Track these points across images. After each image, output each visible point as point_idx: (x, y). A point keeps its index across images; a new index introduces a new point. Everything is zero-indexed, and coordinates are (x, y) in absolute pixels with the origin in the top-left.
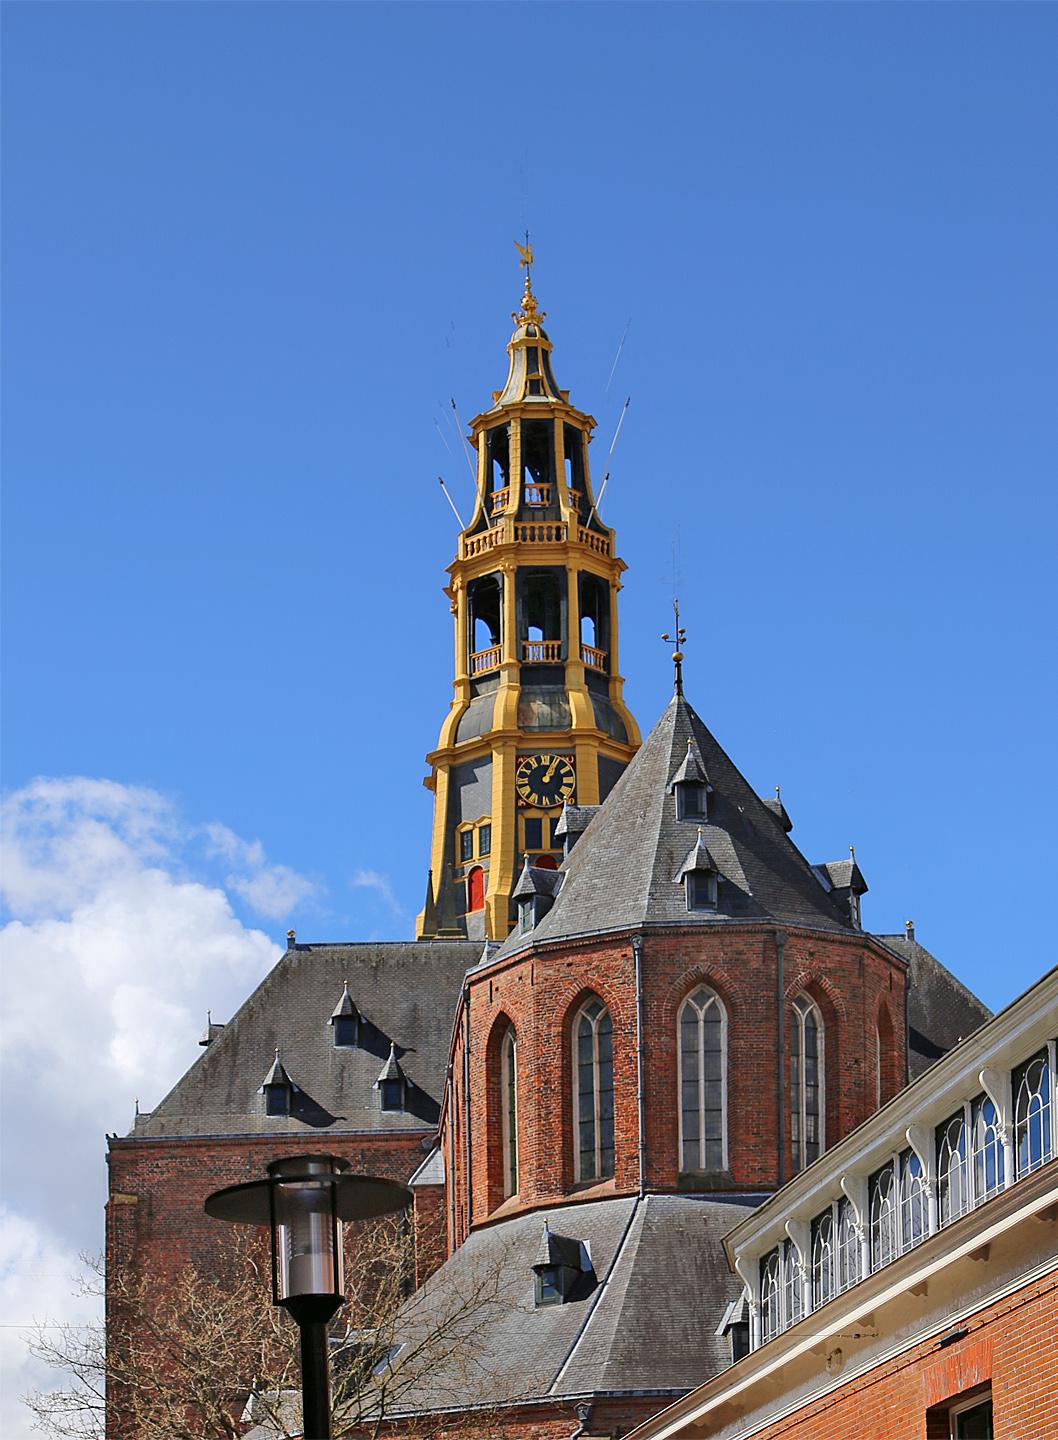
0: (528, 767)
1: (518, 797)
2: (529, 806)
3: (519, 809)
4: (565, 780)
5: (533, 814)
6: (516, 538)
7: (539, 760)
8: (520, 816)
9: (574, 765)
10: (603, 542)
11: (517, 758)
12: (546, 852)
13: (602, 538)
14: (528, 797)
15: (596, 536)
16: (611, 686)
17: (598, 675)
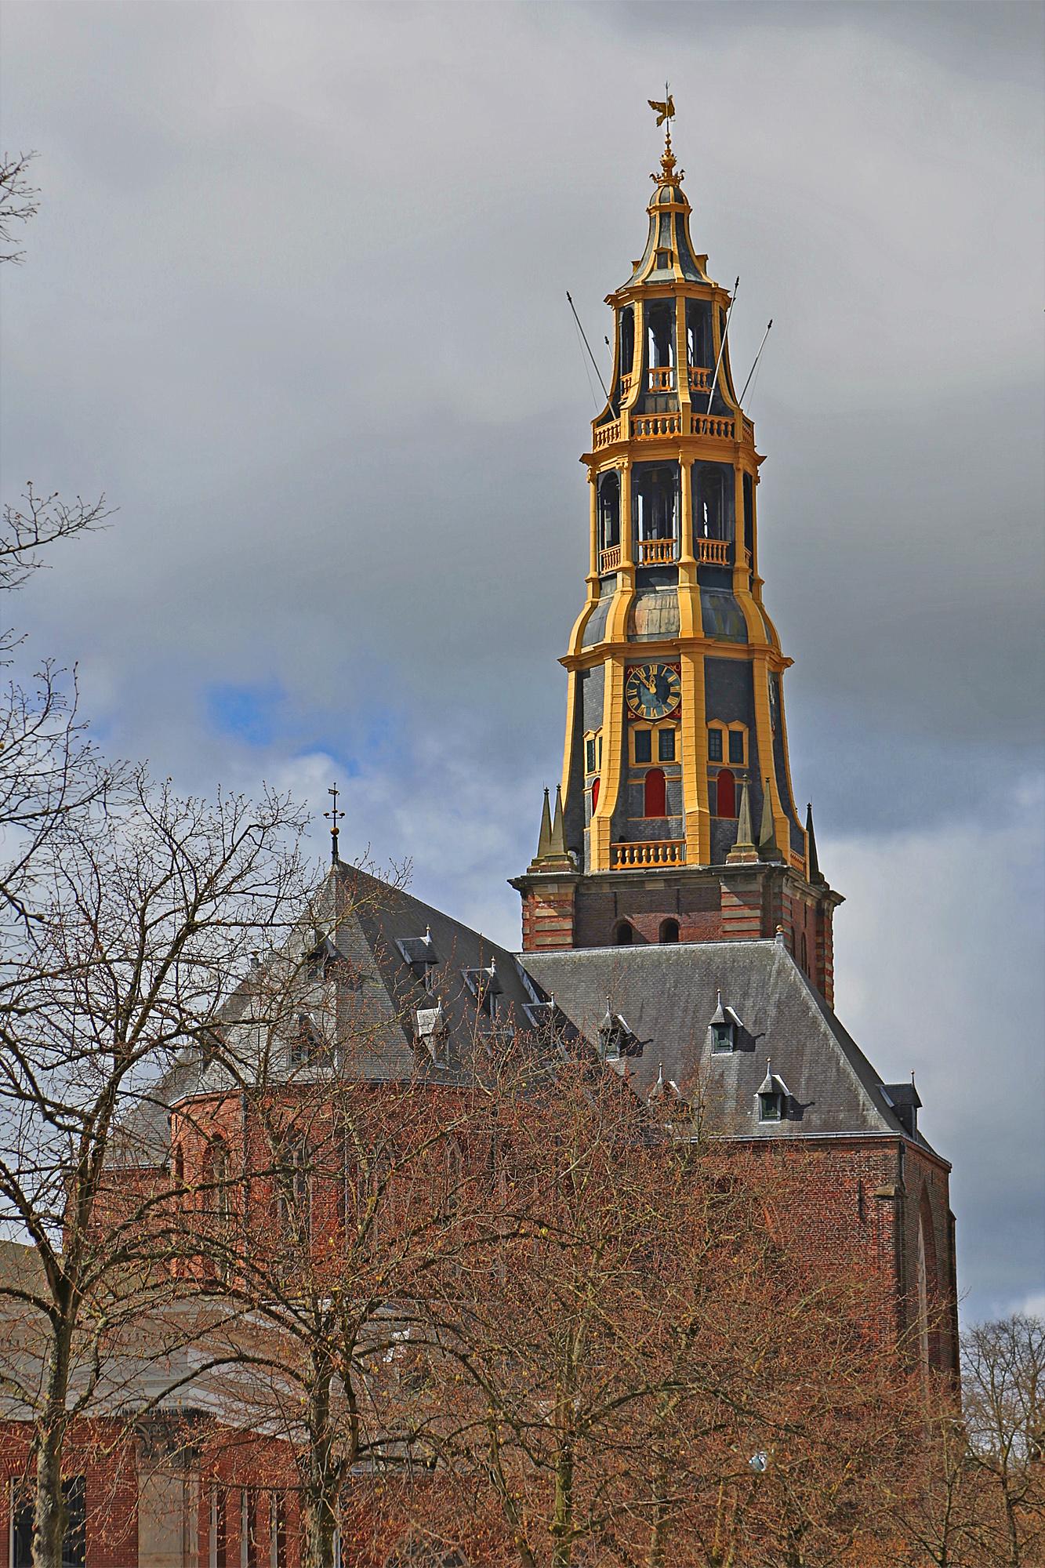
0: (636, 677)
1: (626, 708)
2: (639, 718)
3: (627, 722)
4: (672, 690)
5: (642, 726)
6: (632, 432)
7: (647, 670)
8: (630, 729)
9: (679, 674)
10: (726, 424)
11: (626, 669)
12: (655, 765)
13: (724, 420)
14: (637, 708)
15: (716, 419)
16: (735, 577)
17: (718, 569)
